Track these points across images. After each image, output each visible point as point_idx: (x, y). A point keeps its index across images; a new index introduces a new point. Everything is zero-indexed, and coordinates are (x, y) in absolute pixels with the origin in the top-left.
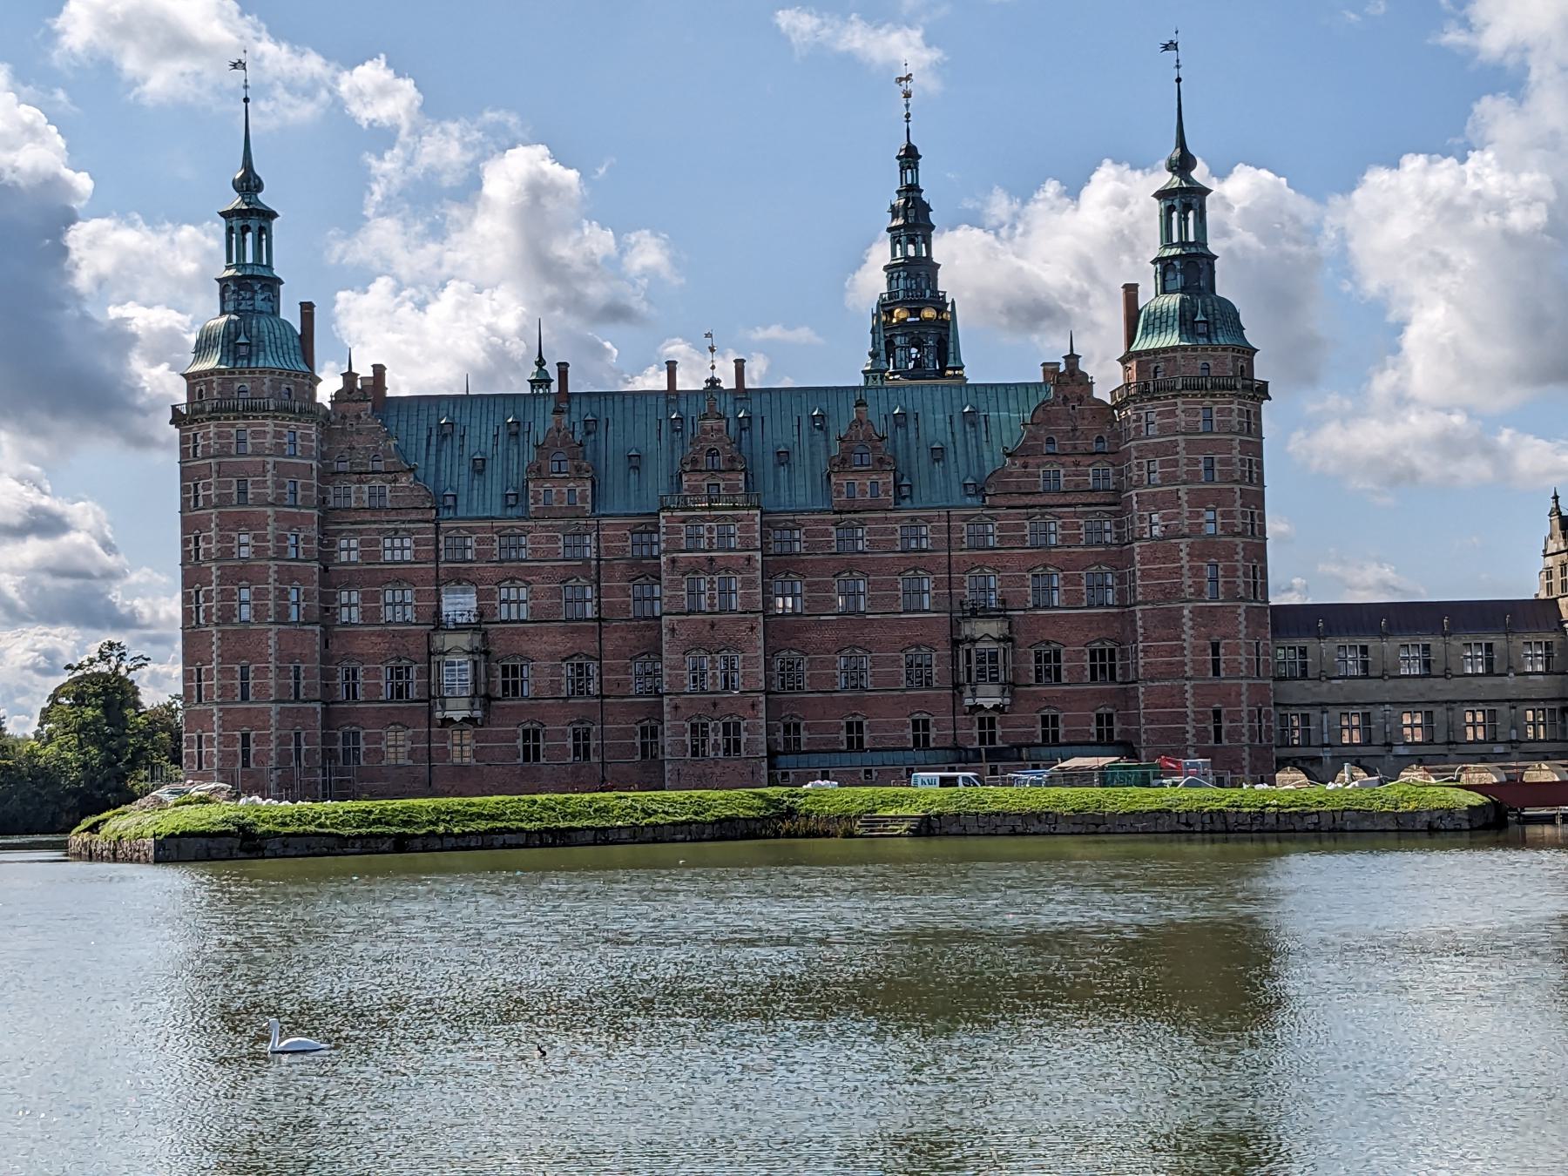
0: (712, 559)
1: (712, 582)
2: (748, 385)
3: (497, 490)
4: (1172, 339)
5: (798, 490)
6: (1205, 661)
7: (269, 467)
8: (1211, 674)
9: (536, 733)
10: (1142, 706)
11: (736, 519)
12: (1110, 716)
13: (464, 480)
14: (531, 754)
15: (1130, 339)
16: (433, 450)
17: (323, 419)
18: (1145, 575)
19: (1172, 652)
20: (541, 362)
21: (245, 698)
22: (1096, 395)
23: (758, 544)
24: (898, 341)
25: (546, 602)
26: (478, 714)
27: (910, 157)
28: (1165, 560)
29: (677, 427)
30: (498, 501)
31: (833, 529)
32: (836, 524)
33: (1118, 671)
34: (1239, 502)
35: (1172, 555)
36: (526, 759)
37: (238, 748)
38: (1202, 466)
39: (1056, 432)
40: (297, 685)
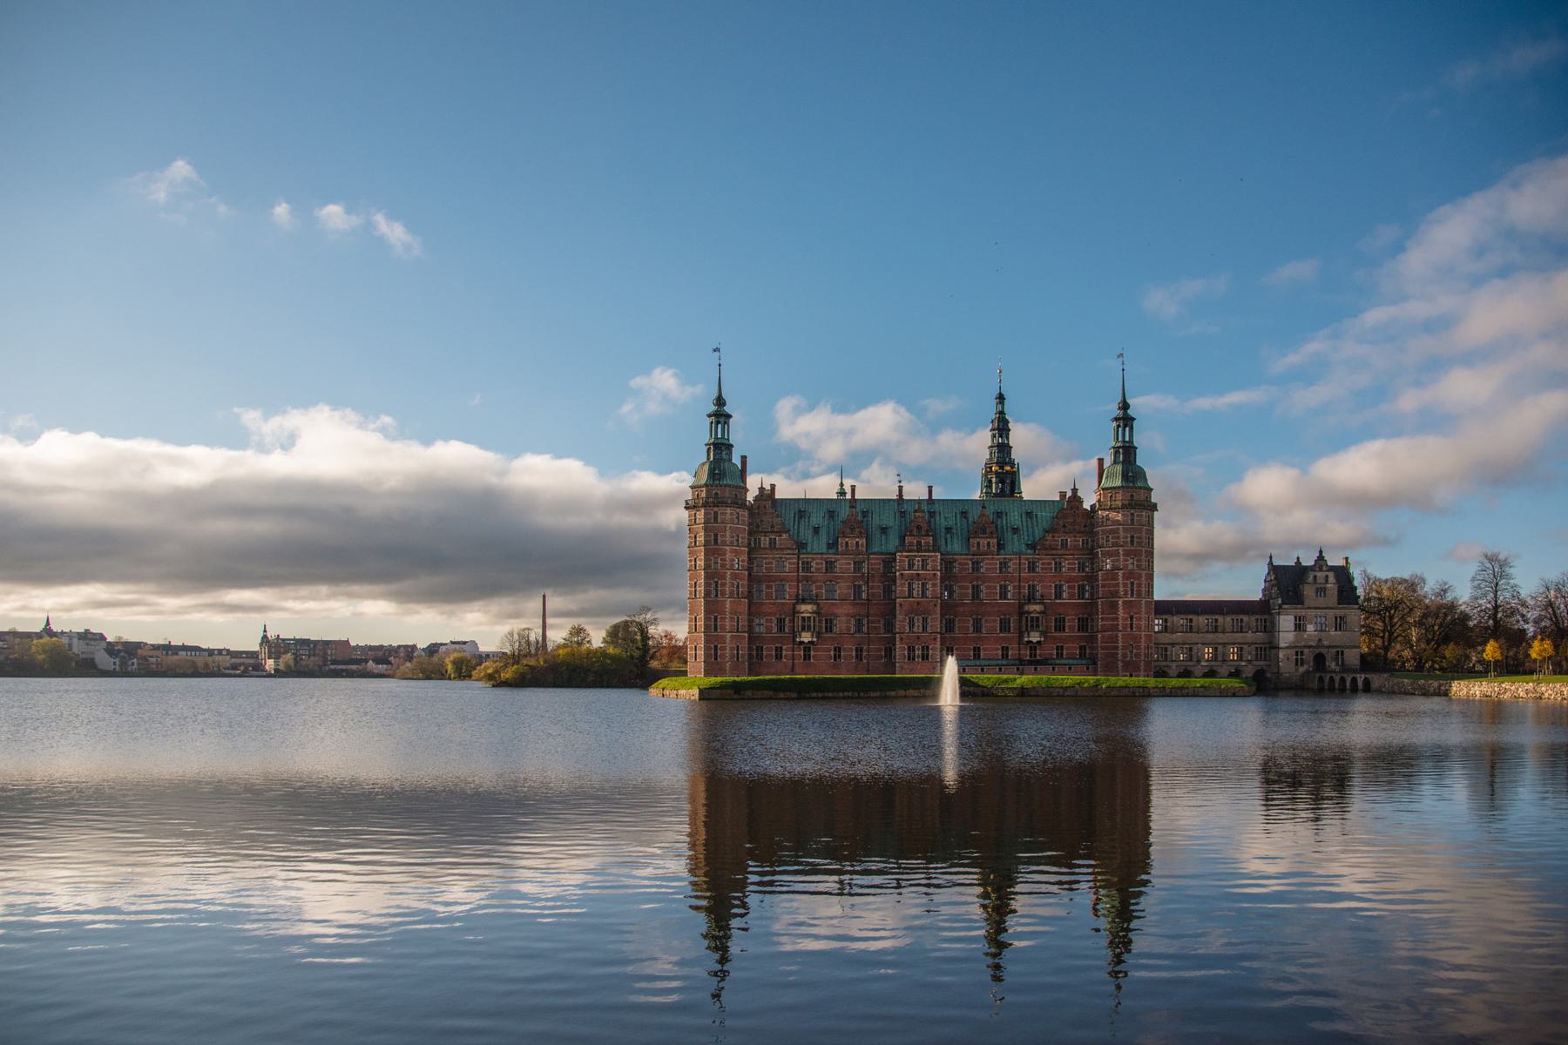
0: (918, 575)
1: (918, 584)
2: (934, 497)
3: (825, 541)
4: (1118, 483)
5: (956, 546)
6: (1127, 624)
7: (728, 528)
8: (1129, 629)
9: (840, 648)
10: (1099, 642)
11: (929, 556)
12: (1085, 646)
13: (810, 536)
15: (1100, 482)
16: (796, 523)
17: (751, 509)
18: (1103, 586)
19: (1113, 619)
21: (716, 629)
23: (939, 568)
25: (845, 591)
26: (815, 639)
28: (1112, 580)
30: (825, 546)
31: (970, 562)
32: (971, 560)
33: (1089, 628)
34: (1144, 555)
35: (1115, 577)
36: (835, 660)
37: (713, 652)
38: (1129, 539)
39: (1067, 522)
40: (738, 625)
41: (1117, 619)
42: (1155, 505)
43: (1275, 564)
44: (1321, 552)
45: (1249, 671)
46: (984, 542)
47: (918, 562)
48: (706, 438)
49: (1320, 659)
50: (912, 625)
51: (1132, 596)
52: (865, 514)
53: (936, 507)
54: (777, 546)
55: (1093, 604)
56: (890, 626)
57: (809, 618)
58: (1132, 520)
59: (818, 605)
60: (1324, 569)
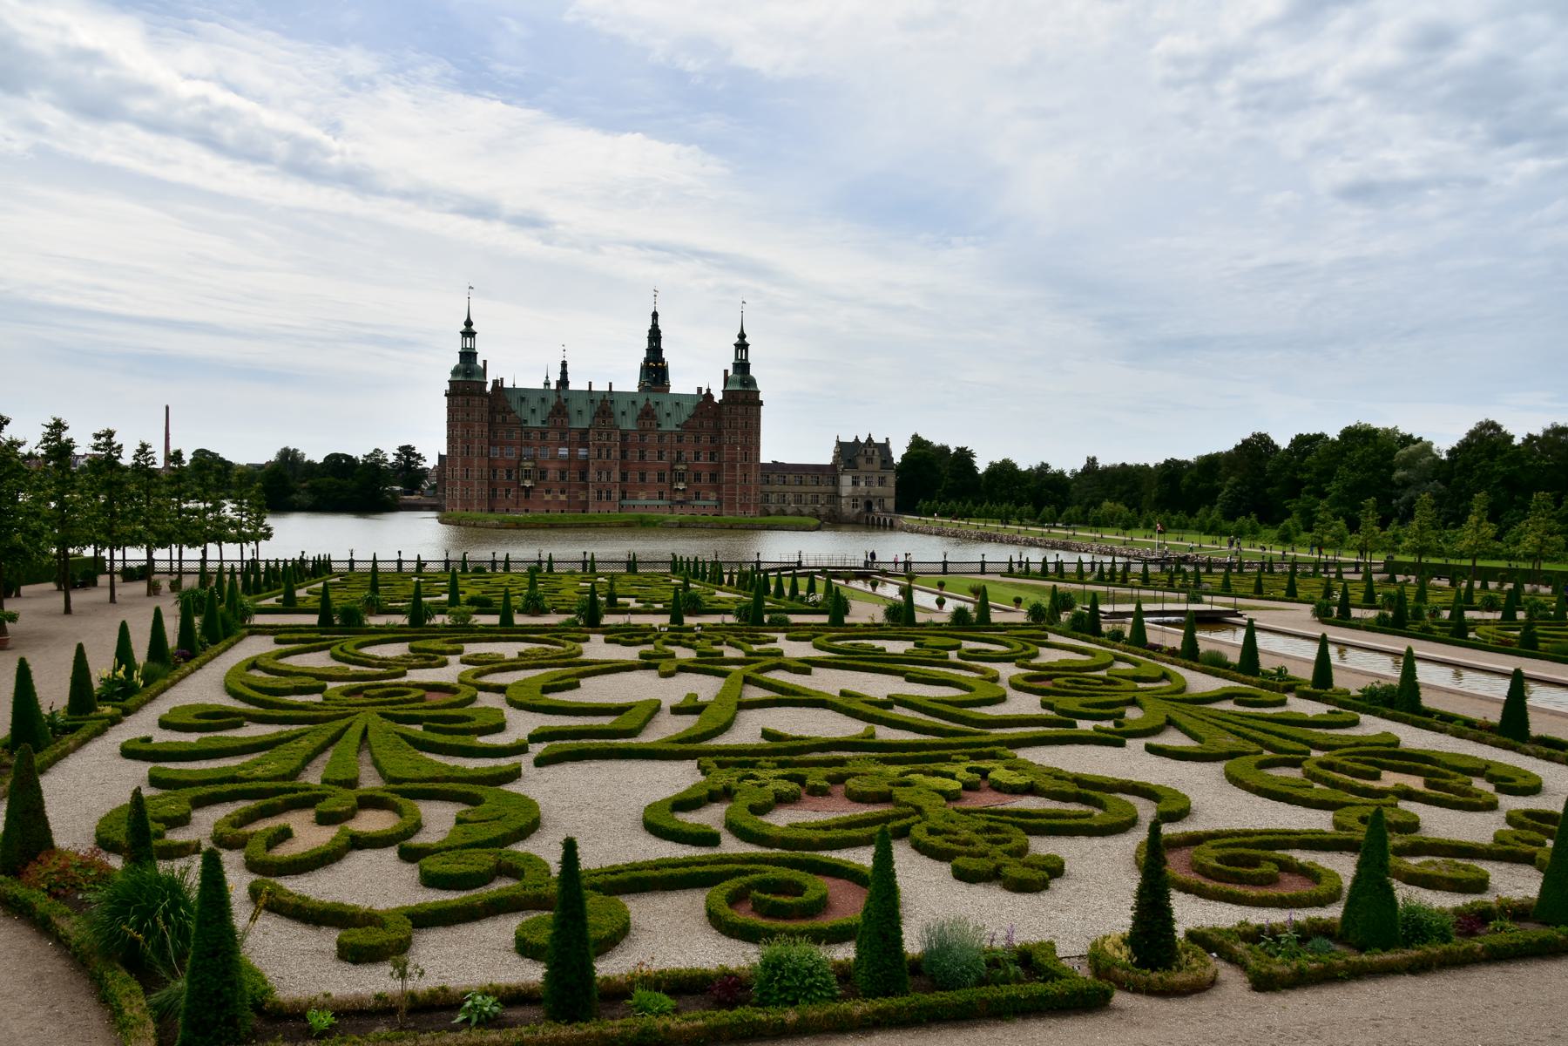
2: (613, 390)
4: (738, 388)
15: (725, 386)
27: (655, 315)
29: (592, 401)
47: (604, 436)
49: (869, 505)
52: (566, 400)
53: (615, 398)
55: (720, 465)
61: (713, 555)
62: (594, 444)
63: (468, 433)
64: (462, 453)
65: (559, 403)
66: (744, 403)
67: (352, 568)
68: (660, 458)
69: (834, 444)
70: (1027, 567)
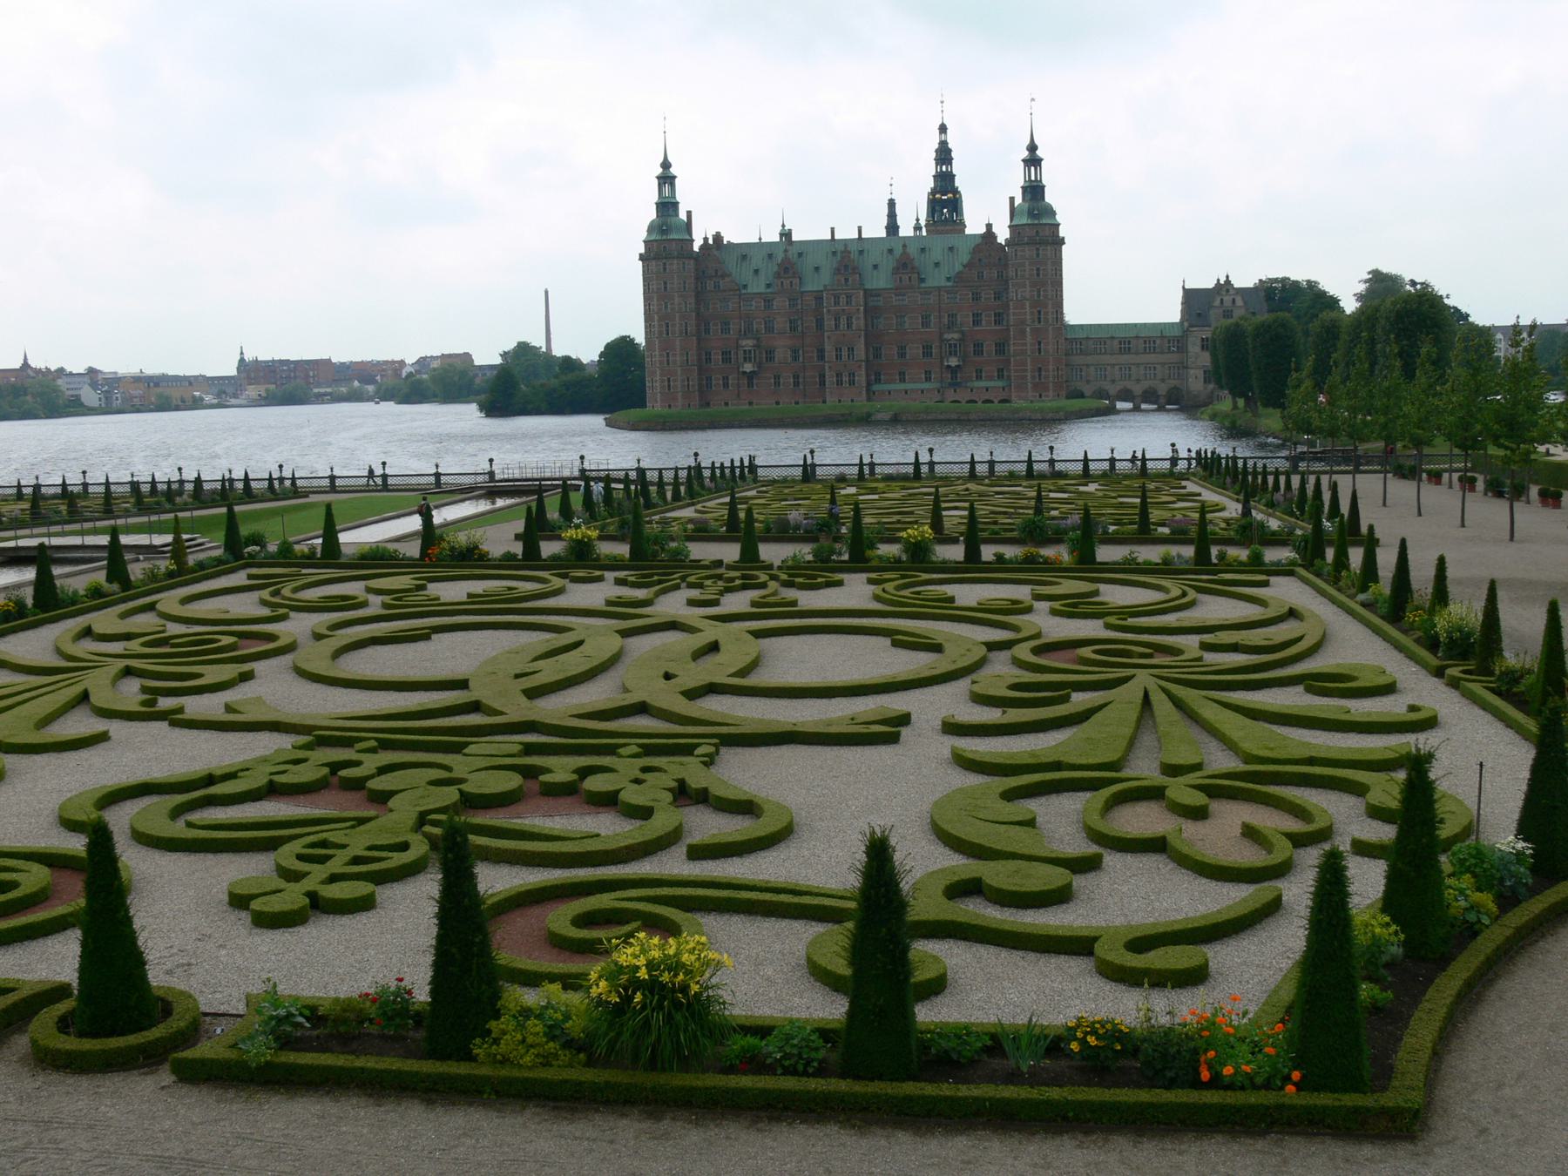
2: (863, 236)
4: (1024, 220)
14: (777, 384)
15: (1011, 220)
20: (783, 226)
22: (999, 241)
24: (937, 208)
27: (943, 129)
29: (834, 253)
30: (763, 286)
37: (666, 383)
41: (1025, 344)
42: (1063, 238)
43: (1186, 287)
44: (1227, 277)
45: (1162, 389)
46: (905, 278)
47: (843, 300)
48: (654, 197)
50: (839, 357)
51: (1039, 322)
52: (800, 255)
54: (721, 288)
55: (1008, 330)
56: (821, 352)
57: (750, 351)
58: (1038, 255)
59: (758, 339)
60: (1232, 292)
61: (692, 459)
62: (829, 311)
63: (666, 307)
64: (660, 333)
65: (786, 260)
66: (1032, 242)
67: (438, 483)
68: (925, 324)
69: (1181, 293)
70: (294, 483)
